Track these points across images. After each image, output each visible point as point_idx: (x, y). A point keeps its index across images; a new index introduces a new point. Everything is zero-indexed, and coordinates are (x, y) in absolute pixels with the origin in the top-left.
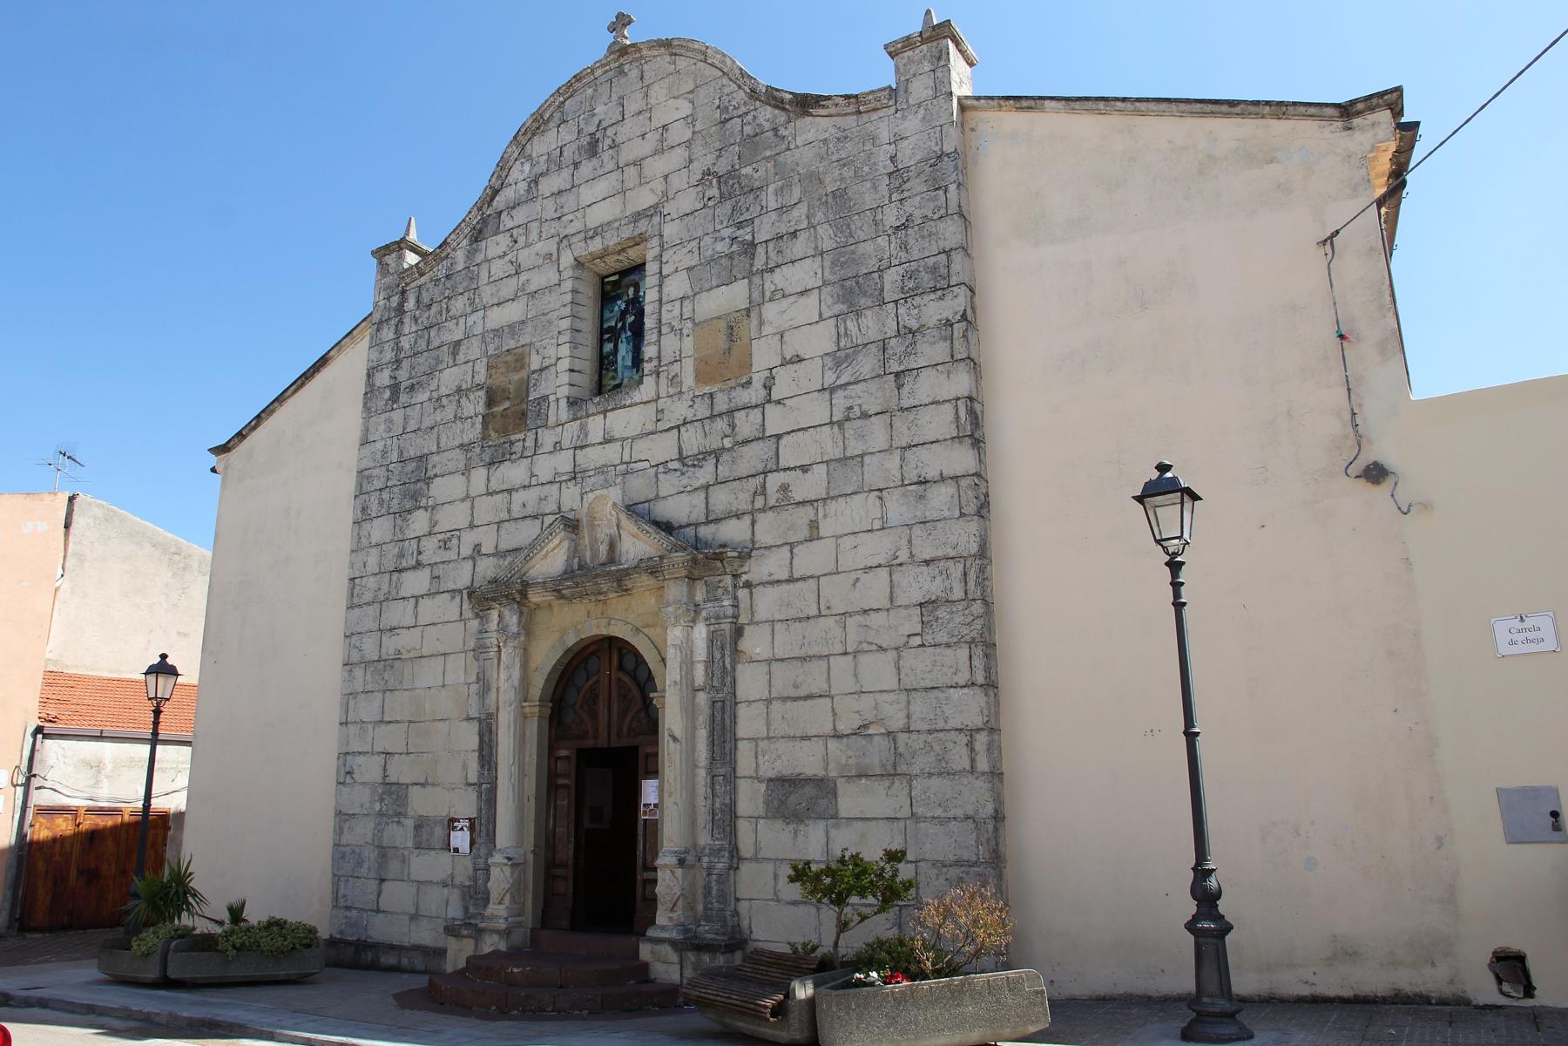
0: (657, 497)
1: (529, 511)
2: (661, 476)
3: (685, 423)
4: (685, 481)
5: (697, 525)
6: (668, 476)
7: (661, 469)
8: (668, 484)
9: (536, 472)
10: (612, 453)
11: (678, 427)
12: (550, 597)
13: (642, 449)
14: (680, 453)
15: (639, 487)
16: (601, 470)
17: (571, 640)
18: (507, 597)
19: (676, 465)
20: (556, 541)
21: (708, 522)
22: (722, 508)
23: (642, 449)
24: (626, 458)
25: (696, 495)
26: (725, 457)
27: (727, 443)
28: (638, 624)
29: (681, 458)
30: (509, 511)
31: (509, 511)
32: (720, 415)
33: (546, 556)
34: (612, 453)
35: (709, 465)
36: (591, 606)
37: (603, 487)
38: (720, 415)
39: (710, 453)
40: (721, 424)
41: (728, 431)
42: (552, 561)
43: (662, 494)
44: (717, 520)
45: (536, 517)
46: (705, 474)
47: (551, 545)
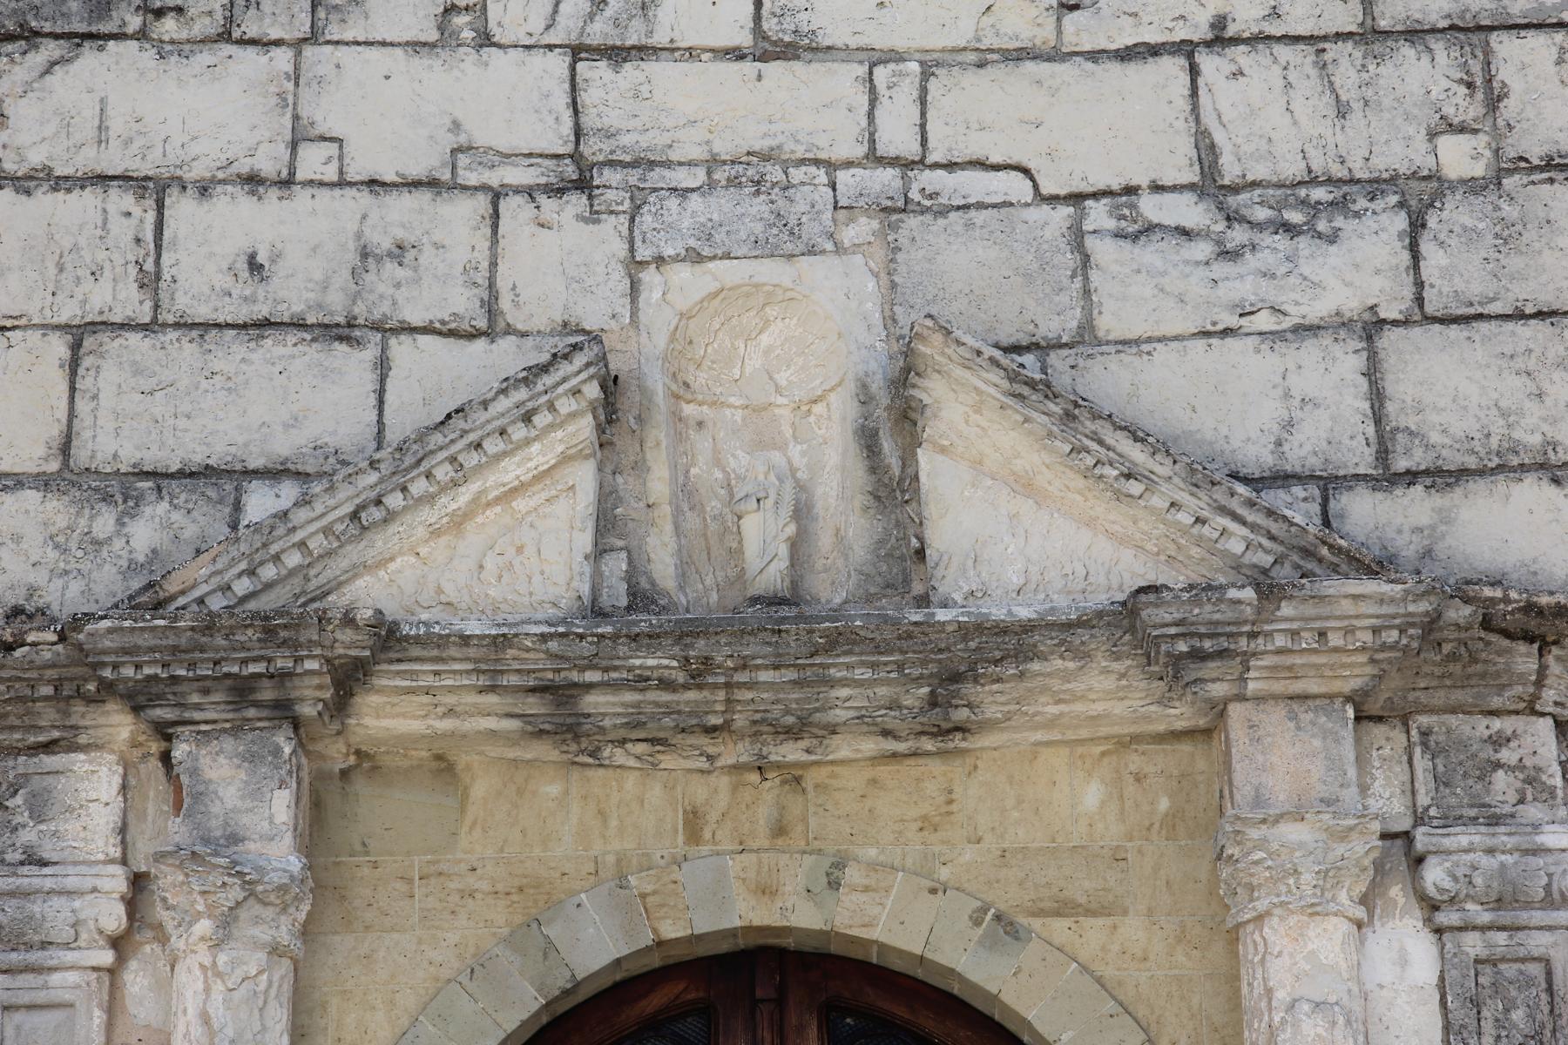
0: (1086, 337)
1: (291, 292)
2: (1103, 250)
3: (1220, 38)
4: (1241, 283)
5: (1329, 484)
6: (1149, 254)
7: (1098, 215)
8: (1141, 289)
9: (326, 113)
10: (810, 108)
11: (1186, 49)
12: (486, 716)
13: (975, 114)
14: (1207, 152)
15: (980, 272)
16: (751, 170)
17: (595, 945)
18: (242, 691)
19: (1188, 211)
20: (540, 456)
21: (1388, 478)
22: (1461, 426)
23: (975, 114)
24: (898, 136)
25: (1310, 351)
26: (1454, 214)
27: (1461, 157)
28: (1005, 898)
29: (1208, 183)
30: (150, 282)
31: (150, 282)
32: (1415, 34)
33: (458, 522)
34: (810, 108)
35: (1375, 239)
36: (714, 793)
37: (764, 249)
38: (1415, 34)
39: (1376, 186)
40: (1425, 76)
41: (1465, 107)
42: (504, 547)
43: (1109, 324)
44: (1441, 477)
45: (341, 332)
46: (1359, 265)
47: (511, 471)
